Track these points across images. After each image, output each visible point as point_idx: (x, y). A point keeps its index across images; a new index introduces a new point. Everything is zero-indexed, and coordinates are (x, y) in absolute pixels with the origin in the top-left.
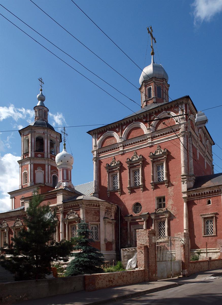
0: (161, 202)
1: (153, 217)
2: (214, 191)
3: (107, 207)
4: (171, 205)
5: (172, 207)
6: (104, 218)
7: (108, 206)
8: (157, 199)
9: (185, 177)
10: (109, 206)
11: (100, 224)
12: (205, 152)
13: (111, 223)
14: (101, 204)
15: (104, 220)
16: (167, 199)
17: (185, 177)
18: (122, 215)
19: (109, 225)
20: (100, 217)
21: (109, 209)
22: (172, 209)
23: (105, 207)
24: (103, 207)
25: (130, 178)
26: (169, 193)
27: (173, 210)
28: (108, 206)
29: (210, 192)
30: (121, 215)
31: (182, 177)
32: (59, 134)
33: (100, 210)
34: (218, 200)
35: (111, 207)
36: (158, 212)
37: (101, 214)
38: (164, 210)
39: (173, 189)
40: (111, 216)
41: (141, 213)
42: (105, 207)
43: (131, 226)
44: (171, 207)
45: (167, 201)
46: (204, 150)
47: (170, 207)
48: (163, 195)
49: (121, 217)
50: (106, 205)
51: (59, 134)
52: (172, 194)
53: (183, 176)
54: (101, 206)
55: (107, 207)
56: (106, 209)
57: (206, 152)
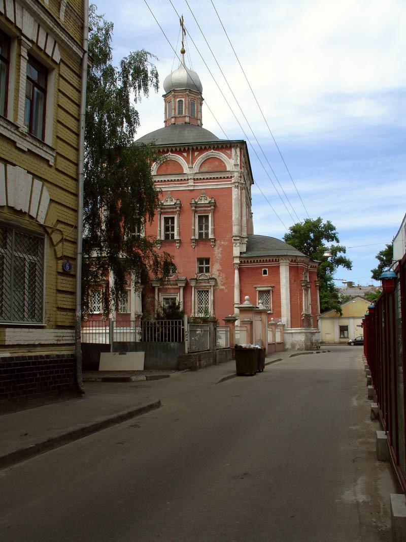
0: (203, 264)
1: (193, 284)
4: (218, 270)
5: (219, 273)
8: (198, 261)
9: (238, 238)
11: (130, 290)
17: (238, 238)
22: (219, 276)
27: (220, 278)
31: (234, 238)
38: (209, 276)
39: (221, 251)
43: (160, 294)
44: (217, 273)
45: (213, 264)
47: (216, 273)
48: (207, 256)
53: (236, 236)
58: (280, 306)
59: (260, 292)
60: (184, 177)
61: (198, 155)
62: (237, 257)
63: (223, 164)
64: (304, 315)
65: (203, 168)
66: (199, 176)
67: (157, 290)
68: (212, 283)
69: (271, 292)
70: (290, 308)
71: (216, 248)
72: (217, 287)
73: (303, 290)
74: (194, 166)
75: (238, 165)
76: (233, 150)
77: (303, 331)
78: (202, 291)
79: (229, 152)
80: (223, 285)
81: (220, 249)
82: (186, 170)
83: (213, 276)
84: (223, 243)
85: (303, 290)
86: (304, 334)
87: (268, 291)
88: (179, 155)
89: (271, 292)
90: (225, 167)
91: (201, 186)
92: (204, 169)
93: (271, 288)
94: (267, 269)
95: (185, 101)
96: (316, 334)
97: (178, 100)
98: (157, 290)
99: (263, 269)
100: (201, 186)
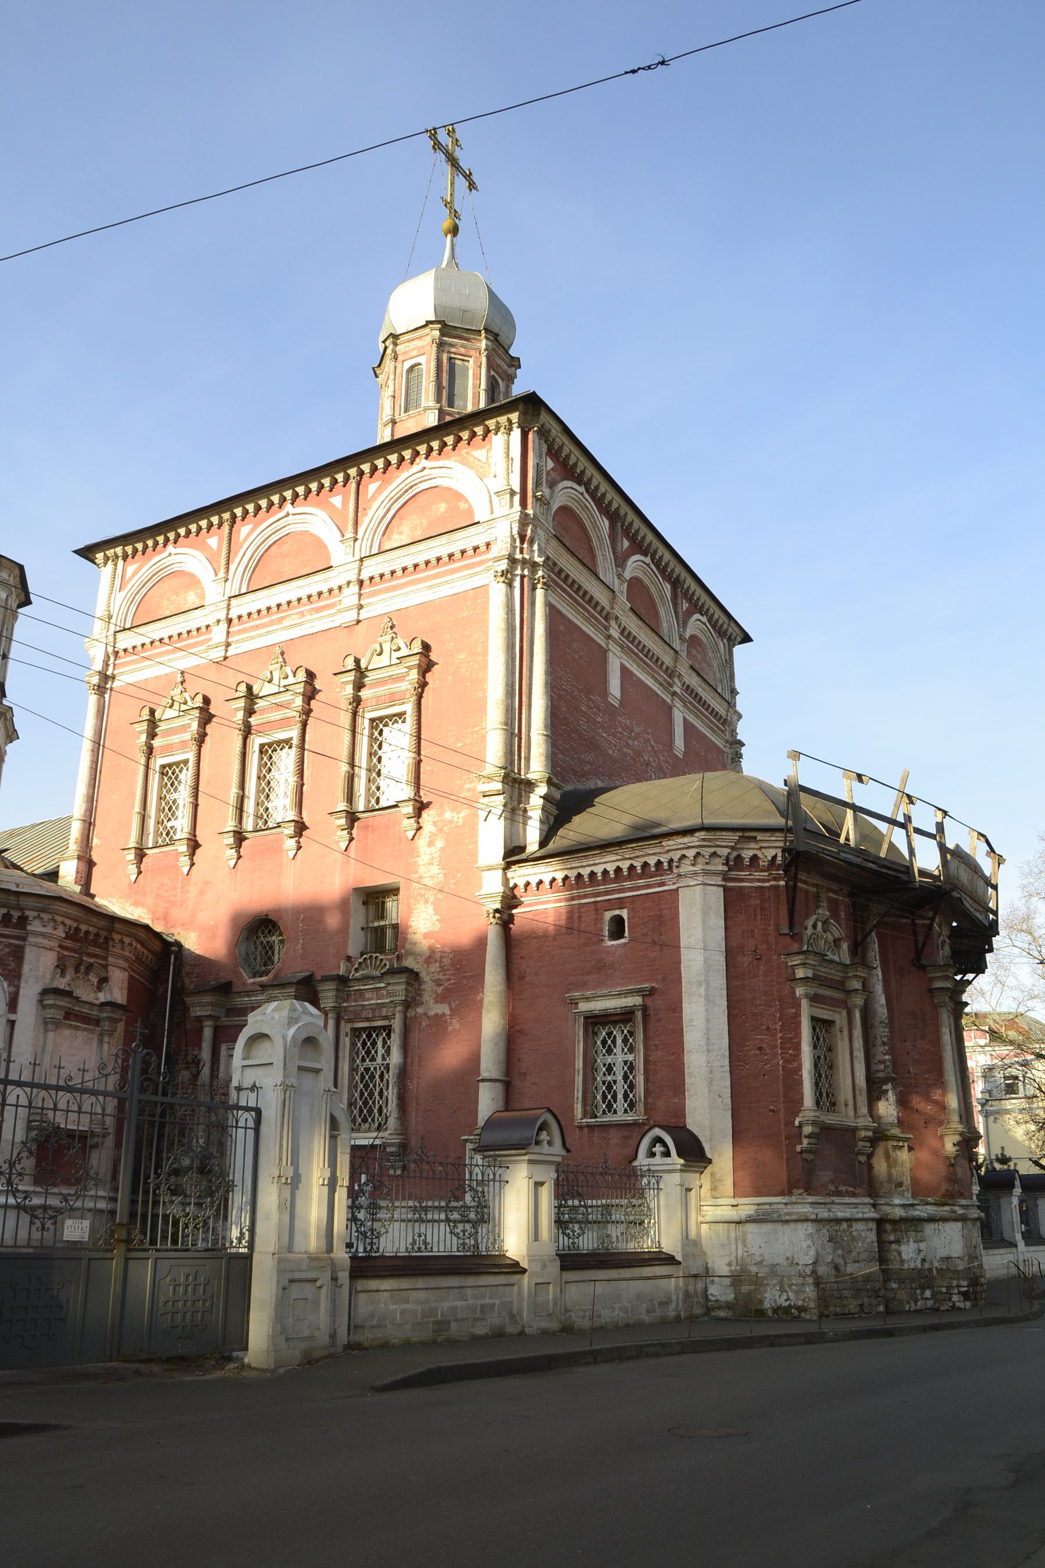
2: (638, 864)
3: (77, 929)
6: (45, 992)
7: (84, 928)
10: (91, 929)
12: (671, 673)
13: (97, 1022)
14: (35, 914)
15: (41, 1001)
16: (409, 905)
18: (187, 980)
19: (79, 1033)
20: (23, 984)
21: (95, 943)
23: (61, 928)
24: (49, 930)
25: (242, 786)
26: (422, 870)
28: (84, 928)
29: (618, 870)
30: (182, 981)
32: (12, 565)
33: (27, 949)
34: (660, 916)
35: (103, 934)
36: (357, 970)
37: (26, 968)
39: (443, 849)
40: (104, 980)
41: (276, 977)
42: (61, 933)
46: (668, 660)
49: (180, 992)
50: (68, 922)
51: (8, 563)
52: (432, 877)
54: (35, 926)
55: (77, 929)
56: (69, 944)
57: (683, 669)
58: (678, 1087)
59: (595, 1021)
60: (325, 580)
61: (380, 490)
62: (491, 868)
63: (463, 506)
64: (807, 1130)
65: (395, 536)
66: (372, 568)
67: (208, 1033)
68: (399, 988)
69: (639, 1014)
70: (727, 1092)
71: (422, 841)
72: (420, 1010)
73: (804, 1003)
74: (360, 536)
75: (513, 493)
76: (498, 440)
77: (805, 1209)
78: (369, 1031)
79: (480, 454)
80: (441, 999)
81: (439, 844)
82: (340, 553)
83: (409, 963)
84: (448, 815)
85: (804, 1003)
86: (810, 1228)
87: (625, 1016)
88: (317, 505)
89: (639, 1014)
90: (470, 511)
91: (380, 604)
92: (396, 540)
93: (637, 1000)
94: (624, 913)
95: (428, 362)
96: (929, 1228)
97: (408, 364)
98: (208, 1033)
99: (608, 915)
100: (380, 604)
